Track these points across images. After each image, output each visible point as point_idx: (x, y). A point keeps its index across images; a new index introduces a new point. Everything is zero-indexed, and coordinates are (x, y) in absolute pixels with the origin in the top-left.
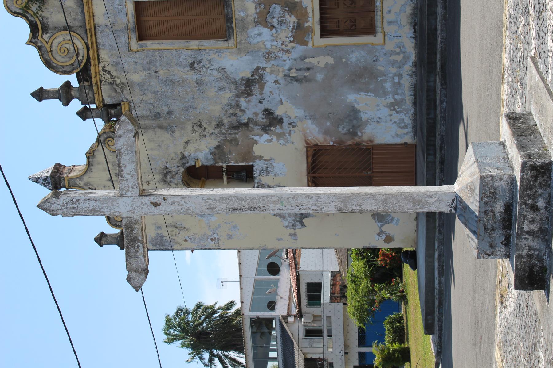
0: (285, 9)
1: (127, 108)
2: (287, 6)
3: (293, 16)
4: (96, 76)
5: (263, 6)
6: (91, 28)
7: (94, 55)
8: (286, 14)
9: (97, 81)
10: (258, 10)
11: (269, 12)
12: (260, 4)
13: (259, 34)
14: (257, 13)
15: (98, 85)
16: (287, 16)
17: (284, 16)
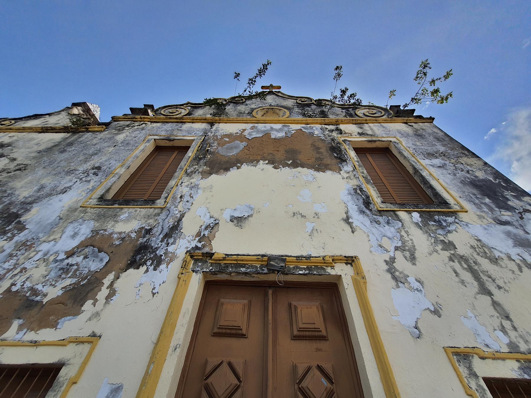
0: (83, 279)
1: (96, 129)
2: (89, 283)
3: (60, 293)
4: (141, 118)
5: (117, 243)
6: (183, 119)
7: (159, 119)
8: (74, 280)
9: (137, 119)
10: (115, 236)
11: (100, 251)
12: (123, 239)
13: (74, 236)
14: (112, 234)
15: (133, 119)
16: (68, 282)
17: (74, 276)
